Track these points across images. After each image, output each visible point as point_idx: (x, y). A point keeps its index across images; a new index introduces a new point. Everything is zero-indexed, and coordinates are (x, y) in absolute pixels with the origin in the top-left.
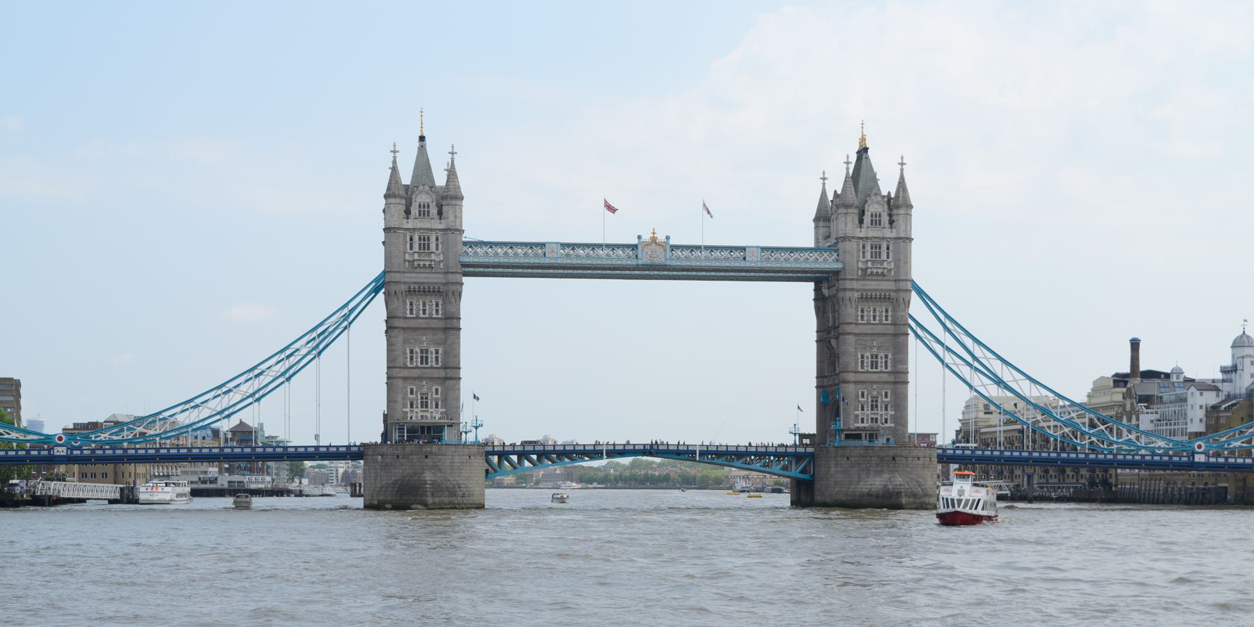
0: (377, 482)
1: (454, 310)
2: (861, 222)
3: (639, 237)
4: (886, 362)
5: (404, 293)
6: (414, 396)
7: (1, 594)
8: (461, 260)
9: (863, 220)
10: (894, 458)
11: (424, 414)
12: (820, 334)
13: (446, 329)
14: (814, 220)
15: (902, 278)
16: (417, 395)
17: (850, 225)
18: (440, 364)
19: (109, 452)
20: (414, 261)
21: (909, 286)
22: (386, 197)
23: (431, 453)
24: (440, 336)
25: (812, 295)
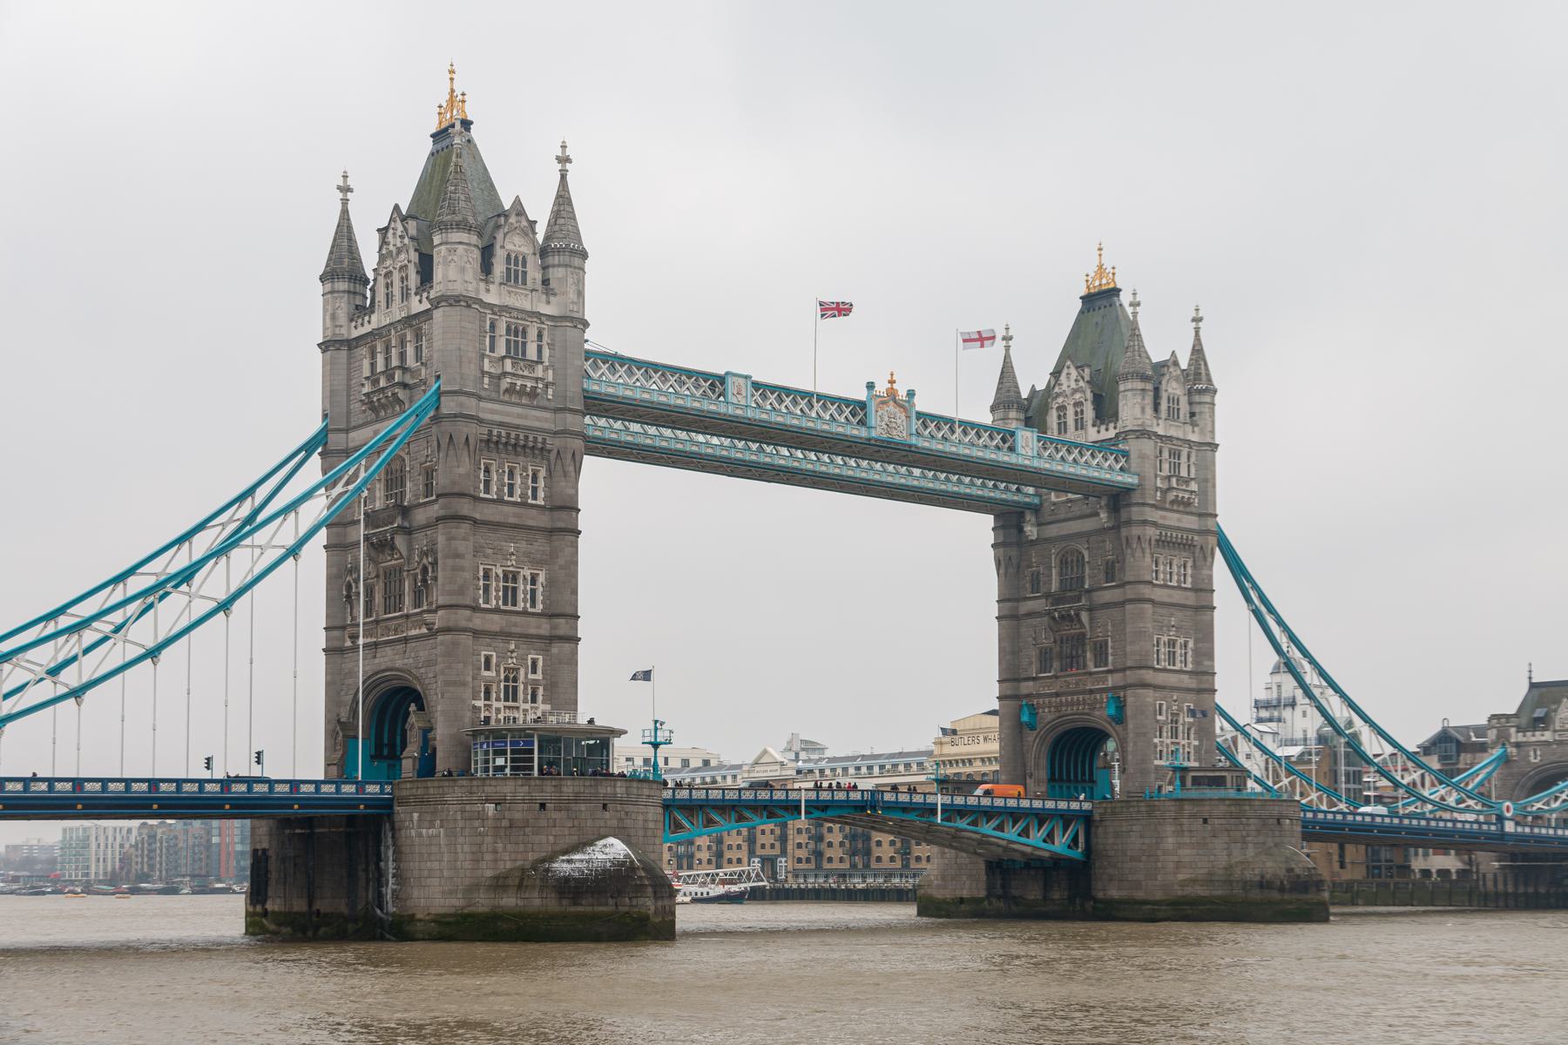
0: (483, 865)
1: (571, 491)
3: (870, 386)
4: (1186, 653)
8: (585, 386)
9: (1159, 404)
11: (509, 713)
12: (1009, 604)
14: (993, 409)
15: (1211, 511)
16: (498, 672)
17: (1149, 411)
18: (539, 607)
20: (505, 374)
21: (1210, 523)
23: (614, 801)
24: (540, 546)
25: (990, 538)
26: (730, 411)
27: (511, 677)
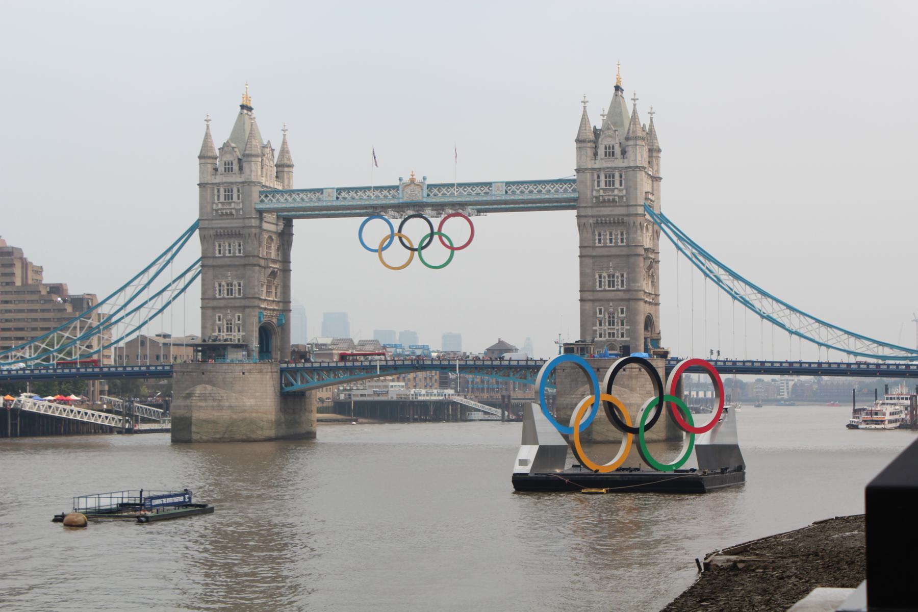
1: (250, 249)
2: (596, 155)
4: (622, 281)
5: (213, 237)
6: (221, 322)
7: (2, 486)
9: (597, 152)
10: (598, 370)
13: (245, 265)
15: (631, 204)
16: (223, 322)
18: (242, 295)
19: (44, 372)
20: (219, 209)
22: (200, 157)
23: (207, 371)
26: (325, 204)
27: (229, 323)
